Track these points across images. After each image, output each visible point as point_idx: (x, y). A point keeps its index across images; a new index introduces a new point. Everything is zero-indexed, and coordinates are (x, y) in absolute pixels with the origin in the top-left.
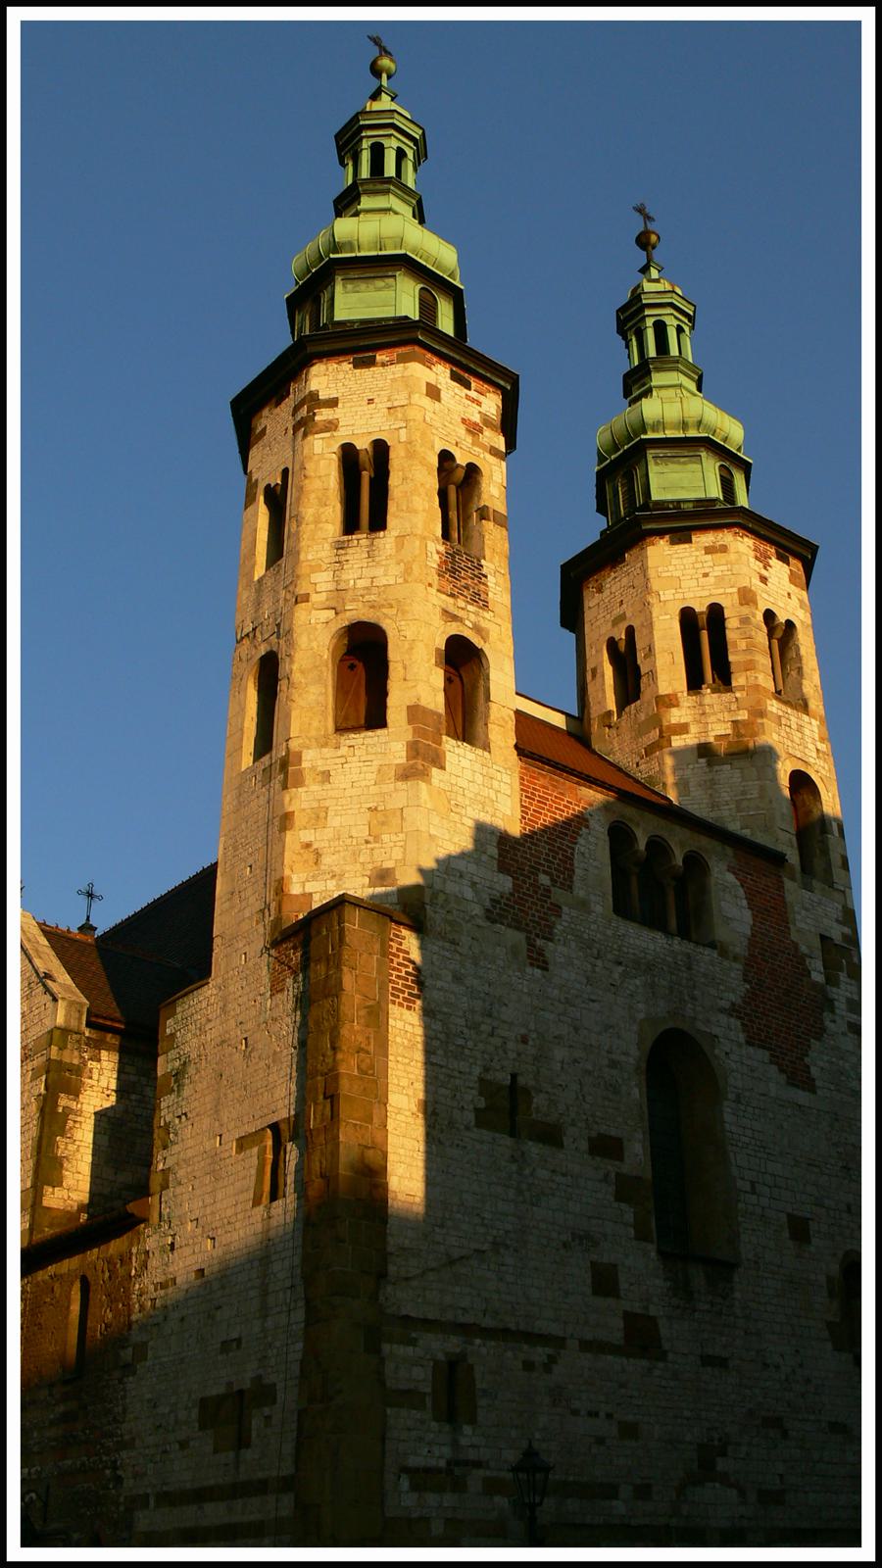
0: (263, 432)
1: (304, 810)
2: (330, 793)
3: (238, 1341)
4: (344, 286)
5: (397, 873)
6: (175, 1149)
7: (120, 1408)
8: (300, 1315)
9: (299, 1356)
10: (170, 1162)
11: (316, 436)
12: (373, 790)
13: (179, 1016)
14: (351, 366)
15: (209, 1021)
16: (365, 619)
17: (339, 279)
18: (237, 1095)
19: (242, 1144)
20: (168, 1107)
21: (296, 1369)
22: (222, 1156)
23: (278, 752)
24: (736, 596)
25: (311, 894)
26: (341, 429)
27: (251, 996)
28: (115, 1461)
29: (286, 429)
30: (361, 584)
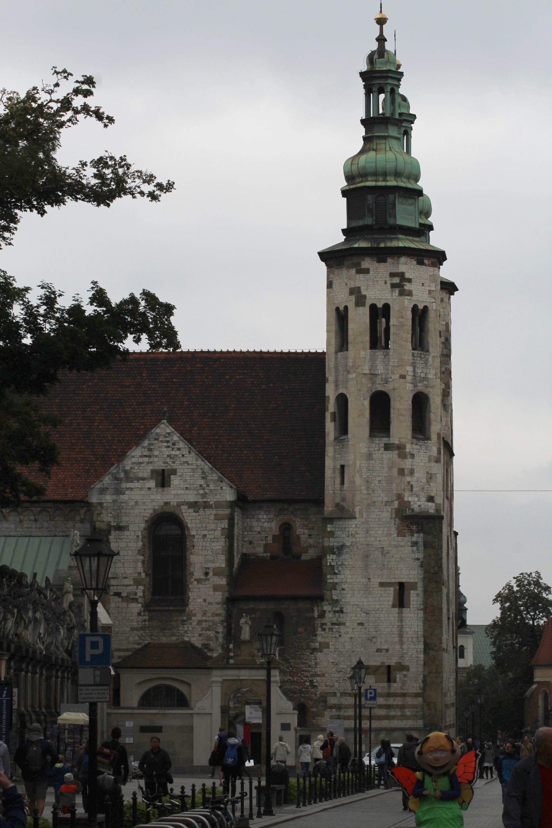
0: (367, 271)
1: (407, 468)
2: (415, 463)
3: (387, 650)
4: (399, 200)
5: (435, 498)
6: (338, 576)
7: (313, 663)
8: (421, 646)
9: (422, 659)
10: (336, 581)
11: (406, 297)
12: (428, 464)
13: (337, 526)
14: (415, 262)
15: (357, 533)
16: (423, 391)
17: (397, 195)
18: (379, 566)
19: (382, 585)
20: (332, 559)
21: (422, 663)
22: (371, 586)
23: (394, 439)
24: (444, 327)
25: (410, 502)
26: (414, 296)
27: (385, 532)
28: (312, 680)
29: (386, 283)
30: (423, 375)
